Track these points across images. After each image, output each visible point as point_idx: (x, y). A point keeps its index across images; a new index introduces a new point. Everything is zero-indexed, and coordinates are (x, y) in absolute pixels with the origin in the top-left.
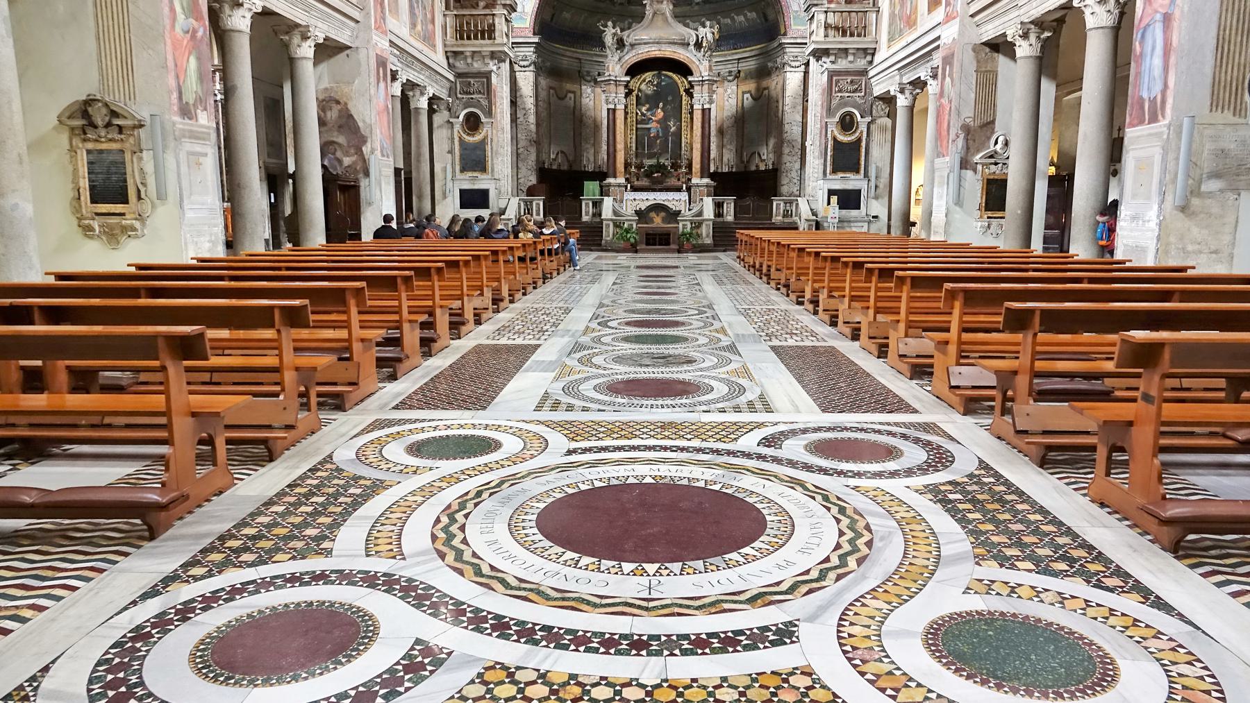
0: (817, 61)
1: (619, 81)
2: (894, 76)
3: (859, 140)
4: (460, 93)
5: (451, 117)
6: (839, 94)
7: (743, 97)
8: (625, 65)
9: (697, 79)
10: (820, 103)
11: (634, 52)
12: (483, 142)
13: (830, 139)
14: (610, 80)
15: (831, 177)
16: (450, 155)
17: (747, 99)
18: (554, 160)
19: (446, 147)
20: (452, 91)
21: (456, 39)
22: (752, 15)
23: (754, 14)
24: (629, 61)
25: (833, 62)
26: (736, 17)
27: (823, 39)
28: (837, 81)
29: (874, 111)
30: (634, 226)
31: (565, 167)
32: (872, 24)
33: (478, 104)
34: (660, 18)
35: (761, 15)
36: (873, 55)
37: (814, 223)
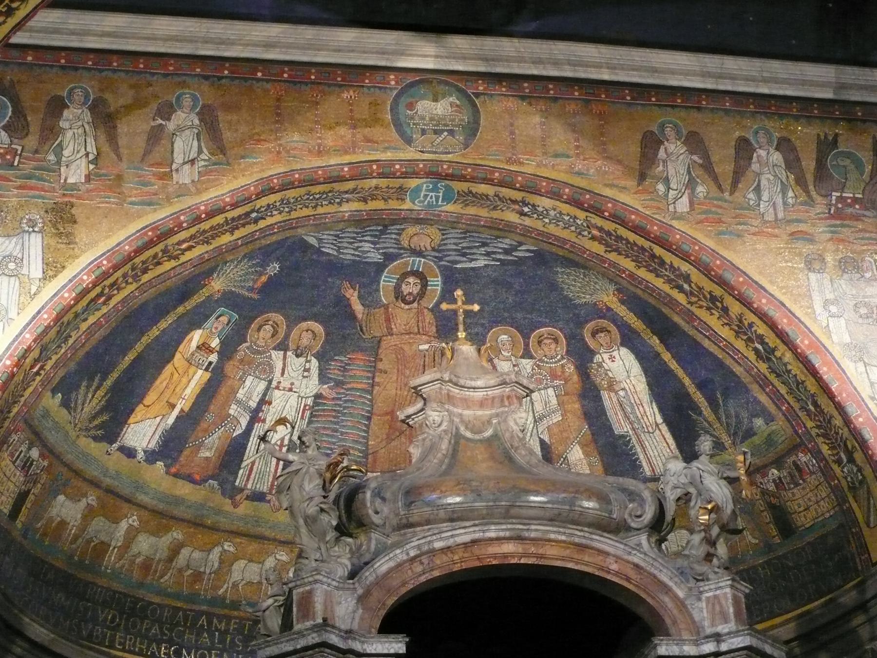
8: (376, 594)
14: (324, 645)
24: (395, 583)
34: (480, 454)
35: (767, 517)
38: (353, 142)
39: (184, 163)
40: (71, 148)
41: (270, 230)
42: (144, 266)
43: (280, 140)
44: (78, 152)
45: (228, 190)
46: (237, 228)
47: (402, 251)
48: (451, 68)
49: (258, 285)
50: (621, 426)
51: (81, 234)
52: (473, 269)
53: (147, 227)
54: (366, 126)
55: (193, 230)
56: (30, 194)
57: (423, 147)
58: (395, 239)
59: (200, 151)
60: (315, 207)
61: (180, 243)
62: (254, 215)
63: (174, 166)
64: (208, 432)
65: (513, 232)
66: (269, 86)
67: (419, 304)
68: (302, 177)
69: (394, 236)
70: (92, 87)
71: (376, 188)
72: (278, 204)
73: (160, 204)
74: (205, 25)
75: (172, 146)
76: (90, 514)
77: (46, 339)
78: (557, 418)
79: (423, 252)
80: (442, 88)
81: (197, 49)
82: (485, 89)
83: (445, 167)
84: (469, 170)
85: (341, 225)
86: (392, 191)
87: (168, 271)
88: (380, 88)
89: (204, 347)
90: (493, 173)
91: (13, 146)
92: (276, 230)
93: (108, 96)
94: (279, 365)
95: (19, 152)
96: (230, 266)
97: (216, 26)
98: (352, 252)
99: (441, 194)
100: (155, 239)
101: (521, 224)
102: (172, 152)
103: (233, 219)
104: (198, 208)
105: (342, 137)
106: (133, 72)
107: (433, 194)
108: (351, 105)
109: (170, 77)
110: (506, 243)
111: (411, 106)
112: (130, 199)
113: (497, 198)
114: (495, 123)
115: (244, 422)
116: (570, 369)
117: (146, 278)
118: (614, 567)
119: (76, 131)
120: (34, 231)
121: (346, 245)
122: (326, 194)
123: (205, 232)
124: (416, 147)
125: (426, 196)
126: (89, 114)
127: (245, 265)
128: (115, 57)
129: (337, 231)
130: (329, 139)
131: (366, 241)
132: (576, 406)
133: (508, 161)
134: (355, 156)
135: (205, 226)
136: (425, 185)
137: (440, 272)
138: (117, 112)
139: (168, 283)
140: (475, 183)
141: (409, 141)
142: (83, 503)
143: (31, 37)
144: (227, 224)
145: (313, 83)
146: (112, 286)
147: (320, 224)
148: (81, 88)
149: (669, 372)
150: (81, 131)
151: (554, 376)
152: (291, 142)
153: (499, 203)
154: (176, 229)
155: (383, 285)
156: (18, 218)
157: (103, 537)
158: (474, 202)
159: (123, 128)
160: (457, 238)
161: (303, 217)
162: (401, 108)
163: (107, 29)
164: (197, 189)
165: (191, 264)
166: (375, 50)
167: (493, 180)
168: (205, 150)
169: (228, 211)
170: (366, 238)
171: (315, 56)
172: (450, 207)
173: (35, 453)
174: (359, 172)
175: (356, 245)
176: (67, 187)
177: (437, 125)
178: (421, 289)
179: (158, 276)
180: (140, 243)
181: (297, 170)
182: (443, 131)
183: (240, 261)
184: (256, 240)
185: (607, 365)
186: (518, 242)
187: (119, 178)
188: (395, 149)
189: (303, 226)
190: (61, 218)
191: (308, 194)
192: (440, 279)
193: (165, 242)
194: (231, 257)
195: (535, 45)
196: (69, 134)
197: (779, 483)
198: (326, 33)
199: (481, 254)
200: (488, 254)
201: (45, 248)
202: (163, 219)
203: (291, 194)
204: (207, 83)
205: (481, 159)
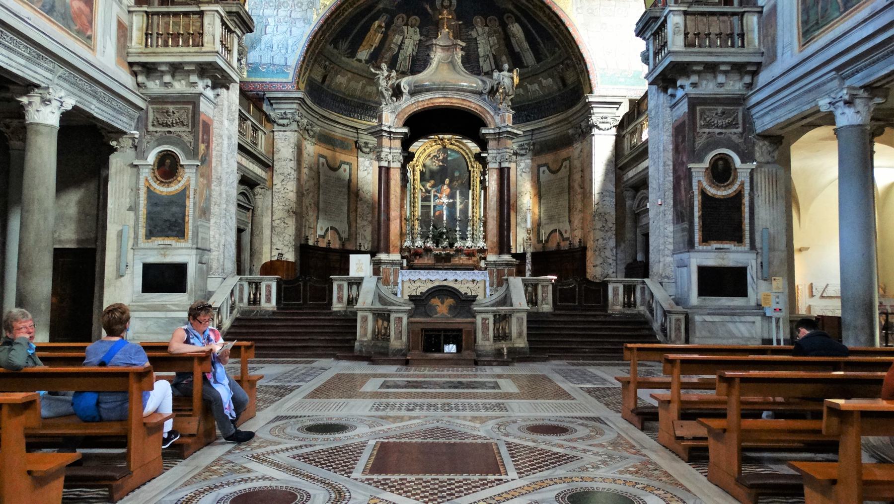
0: (665, 90)
1: (394, 133)
2: (824, 84)
3: (739, 195)
4: (153, 125)
5: (137, 158)
6: (707, 130)
7: (539, 170)
8: (402, 114)
9: (492, 131)
10: (671, 147)
11: (413, 100)
12: (183, 195)
13: (696, 192)
15: (701, 248)
16: (132, 214)
17: (544, 171)
18: (323, 237)
19: (127, 202)
20: (141, 123)
21: (146, 46)
22: (548, 82)
23: (550, 80)
24: (407, 111)
25: (694, 85)
26: (529, 86)
27: (683, 49)
28: (702, 113)
29: (757, 155)
30: (405, 321)
31: (336, 245)
32: (753, 31)
33: (179, 142)
35: (559, 80)
36: (755, 74)
37: (682, 317)
50: (517, 50)
64: (385, 53)
76: (349, 81)
77: (323, 29)
78: (497, 46)
89: (380, 26)
94: (406, 31)
115: (397, 50)
116: (500, 30)
117: (355, 6)
118: (473, 106)
132: (502, 42)
142: (346, 77)
146: (343, 10)
149: (530, 30)
151: (495, 32)
157: (354, 87)
173: (327, 63)
185: (512, 28)
197: (562, 69)
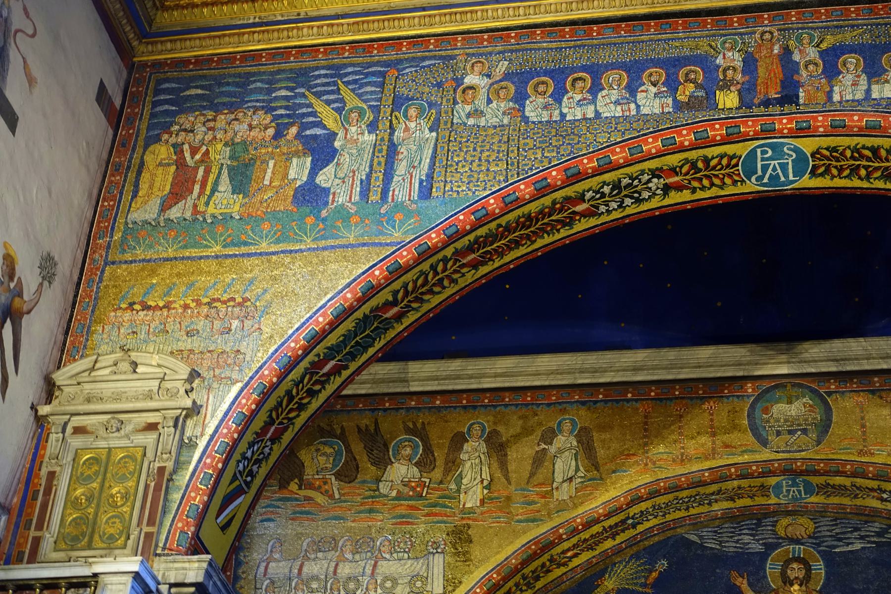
38: (713, 449)
39: (564, 481)
40: (469, 476)
41: (650, 532)
42: (535, 575)
43: (647, 453)
44: (475, 479)
45: (601, 502)
46: (618, 534)
47: (780, 541)
48: (805, 371)
49: (651, 580)
51: (476, 552)
52: (850, 551)
53: (530, 541)
54: (725, 433)
55: (574, 540)
56: (435, 520)
57: (779, 447)
58: (771, 530)
59: (577, 469)
60: (687, 509)
61: (564, 552)
62: (630, 521)
63: (555, 485)
65: (880, 516)
66: (638, 405)
67: (807, 587)
68: (667, 485)
69: (770, 528)
70: (488, 422)
71: (739, 488)
72: (651, 510)
73: (542, 520)
74: (579, 358)
75: (554, 467)
79: (800, 540)
80: (795, 392)
81: (575, 378)
82: (837, 387)
83: (799, 464)
84: (822, 465)
85: (717, 523)
86: (755, 489)
87: (560, 576)
88: (738, 397)
90: (844, 466)
91: (422, 479)
92: (656, 532)
93: (501, 429)
95: (427, 484)
96: (619, 566)
97: (589, 357)
98: (734, 545)
99: (802, 488)
100: (539, 551)
101: (884, 509)
102: (554, 472)
103: (611, 527)
104: (575, 521)
105: (703, 445)
106: (522, 404)
107: (795, 489)
108: (712, 415)
109: (552, 406)
110: (876, 526)
111: (766, 410)
112: (517, 518)
113: (855, 488)
114: (846, 418)
117: (539, 585)
119: (473, 461)
120: (437, 552)
121: (726, 539)
122: (694, 497)
123: (586, 540)
124: (772, 448)
125: (788, 491)
126: (485, 445)
127: (633, 566)
128: (507, 394)
129: (714, 527)
130: (692, 447)
131: (744, 534)
133: (859, 453)
134: (714, 461)
135: (586, 535)
136: (784, 482)
137: (821, 556)
138: (508, 441)
139: (563, 586)
140: (830, 476)
141: (764, 443)
143: (439, 384)
144: (606, 533)
145: (677, 398)
147: (696, 524)
148: (478, 423)
150: (477, 461)
152: (657, 454)
153: (858, 492)
154: (556, 541)
155: (769, 572)
156: (425, 542)
158: (834, 492)
159: (513, 454)
160: (829, 525)
161: (678, 519)
162: (758, 413)
163: (499, 371)
164: (574, 504)
165: (581, 568)
166: (731, 363)
167: (845, 472)
168: (581, 468)
169: (603, 521)
170: (744, 532)
171: (679, 373)
172: (813, 499)
174: (720, 476)
175: (736, 538)
176: (464, 511)
177: (792, 426)
178: (806, 574)
179: (552, 582)
180: (525, 556)
181: (662, 479)
182: (797, 430)
183: (628, 562)
184: (639, 541)
186: (886, 525)
187: (508, 498)
188: (751, 451)
189: (682, 526)
190: (460, 538)
191: (677, 499)
192: (822, 563)
193: (550, 553)
194: (619, 559)
195: (882, 342)
196: (468, 464)
198: (686, 352)
199: (855, 538)
200: (862, 538)
201: (447, 566)
202: (544, 533)
203: (661, 500)
204: (583, 407)
205: (833, 453)
